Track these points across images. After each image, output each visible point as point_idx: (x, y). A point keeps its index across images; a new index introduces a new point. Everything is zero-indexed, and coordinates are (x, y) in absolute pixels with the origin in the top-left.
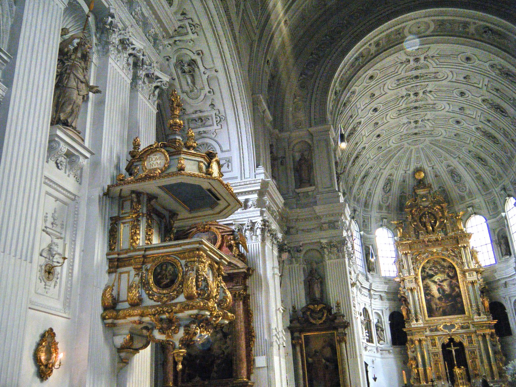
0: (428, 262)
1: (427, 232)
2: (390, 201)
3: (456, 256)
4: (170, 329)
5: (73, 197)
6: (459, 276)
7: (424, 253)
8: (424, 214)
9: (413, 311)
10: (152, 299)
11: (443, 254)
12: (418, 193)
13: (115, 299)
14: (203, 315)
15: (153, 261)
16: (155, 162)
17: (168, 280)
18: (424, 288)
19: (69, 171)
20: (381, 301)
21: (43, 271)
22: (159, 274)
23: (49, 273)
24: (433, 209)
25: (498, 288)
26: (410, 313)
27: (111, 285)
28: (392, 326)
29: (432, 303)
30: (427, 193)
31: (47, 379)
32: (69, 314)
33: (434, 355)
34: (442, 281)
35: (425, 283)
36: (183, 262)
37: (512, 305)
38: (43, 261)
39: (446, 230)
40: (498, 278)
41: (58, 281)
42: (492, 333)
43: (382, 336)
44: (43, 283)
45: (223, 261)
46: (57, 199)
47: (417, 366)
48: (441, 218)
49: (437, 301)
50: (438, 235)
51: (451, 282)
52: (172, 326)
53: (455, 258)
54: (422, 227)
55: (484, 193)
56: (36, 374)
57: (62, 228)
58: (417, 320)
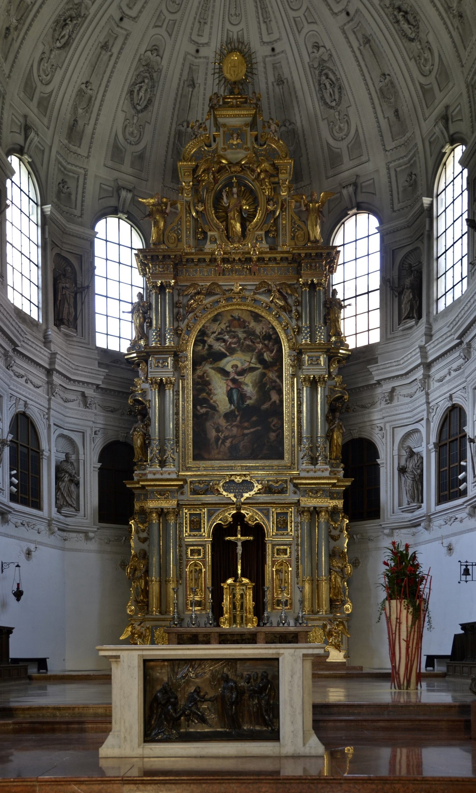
0: (215, 319)
1: (228, 237)
2: (147, 138)
3: (286, 309)
6: (286, 361)
7: (209, 293)
8: (229, 184)
9: (155, 443)
11: (255, 300)
12: (221, 120)
18: (195, 383)
20: (82, 408)
24: (253, 171)
25: (373, 404)
26: (149, 443)
28: (102, 473)
29: (209, 424)
30: (246, 125)
33: (193, 552)
34: (242, 373)
35: (199, 372)
37: (396, 447)
39: (275, 237)
40: (376, 378)
42: (335, 508)
43: (71, 497)
47: (147, 572)
48: (269, 200)
49: (222, 422)
50: (254, 246)
51: (263, 375)
53: (284, 313)
54: (216, 220)
55: (390, 145)
58: (163, 464)
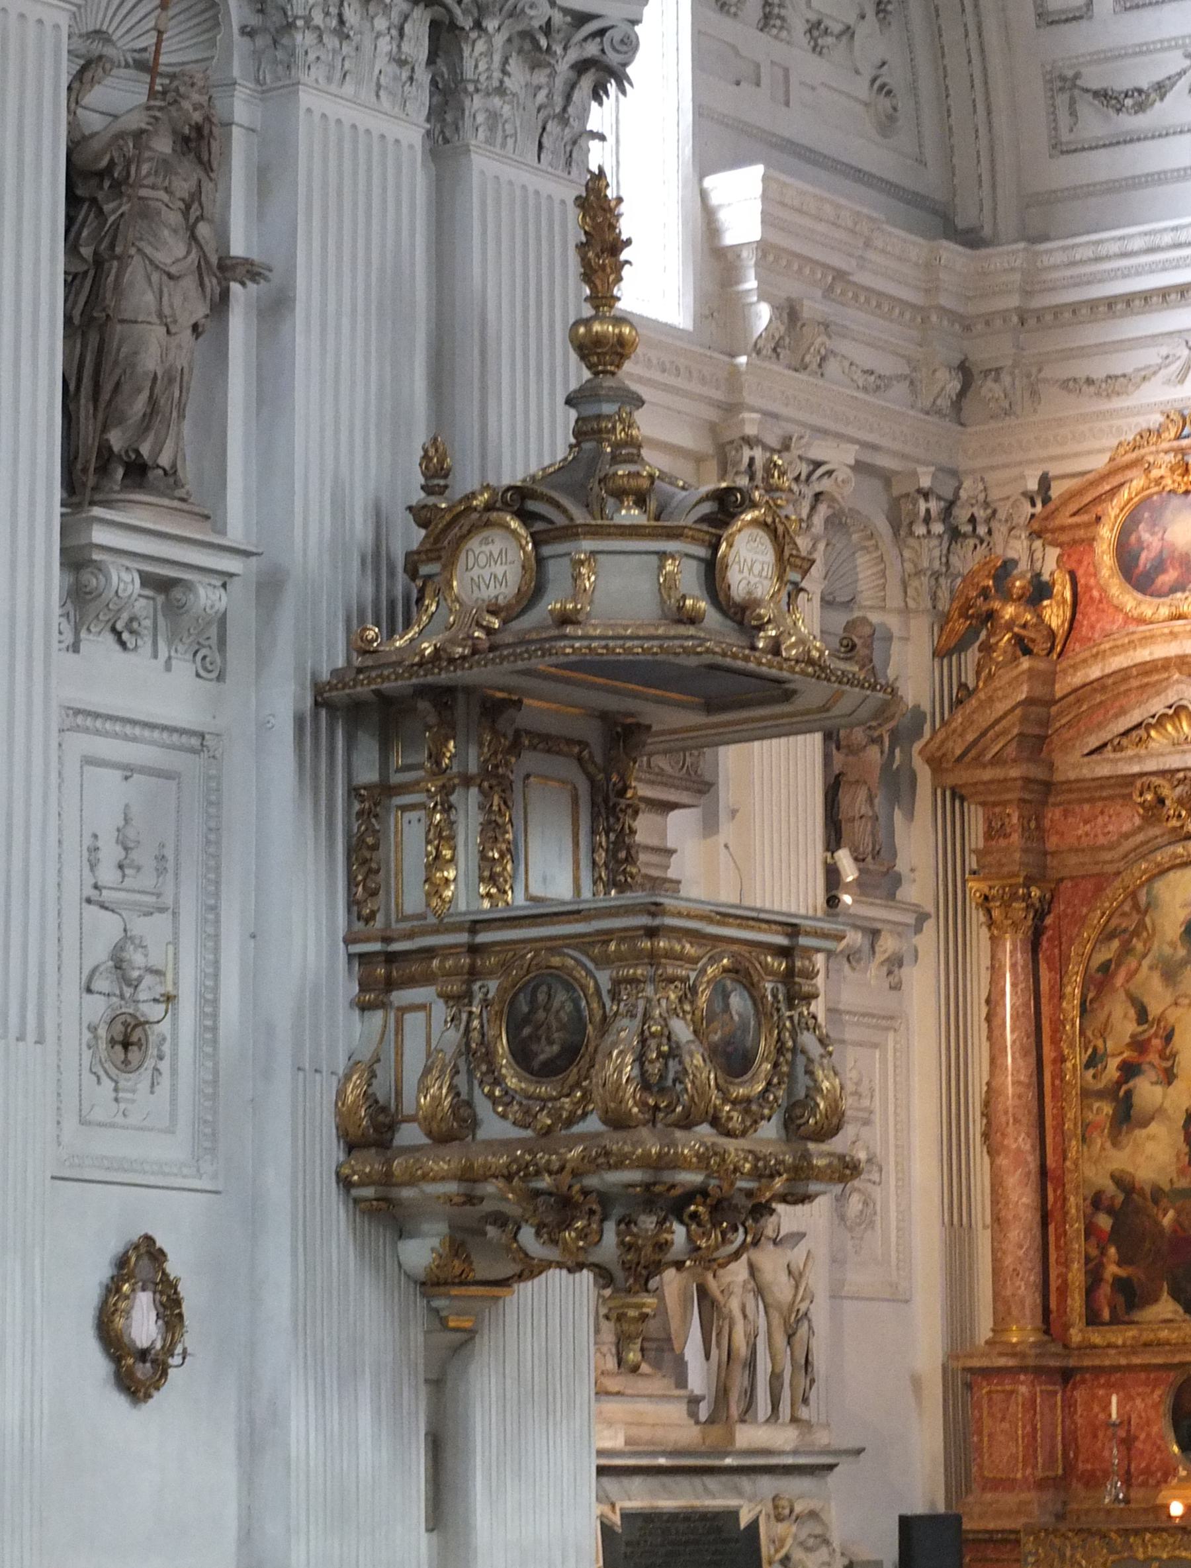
4: (568, 1227)
5: (195, 742)
10: (504, 1116)
13: (384, 1109)
14: (673, 1186)
15: (505, 966)
16: (486, 573)
17: (556, 1048)
19: (170, 643)
21: (103, 1045)
22: (527, 1020)
23: (126, 1045)
27: (366, 1055)
31: (150, 1396)
32: (215, 1177)
36: (604, 978)
38: (97, 1008)
41: (164, 1066)
44: (108, 1084)
45: (803, 941)
46: (129, 771)
52: (574, 1219)
56: (112, 1381)
57: (161, 872)
